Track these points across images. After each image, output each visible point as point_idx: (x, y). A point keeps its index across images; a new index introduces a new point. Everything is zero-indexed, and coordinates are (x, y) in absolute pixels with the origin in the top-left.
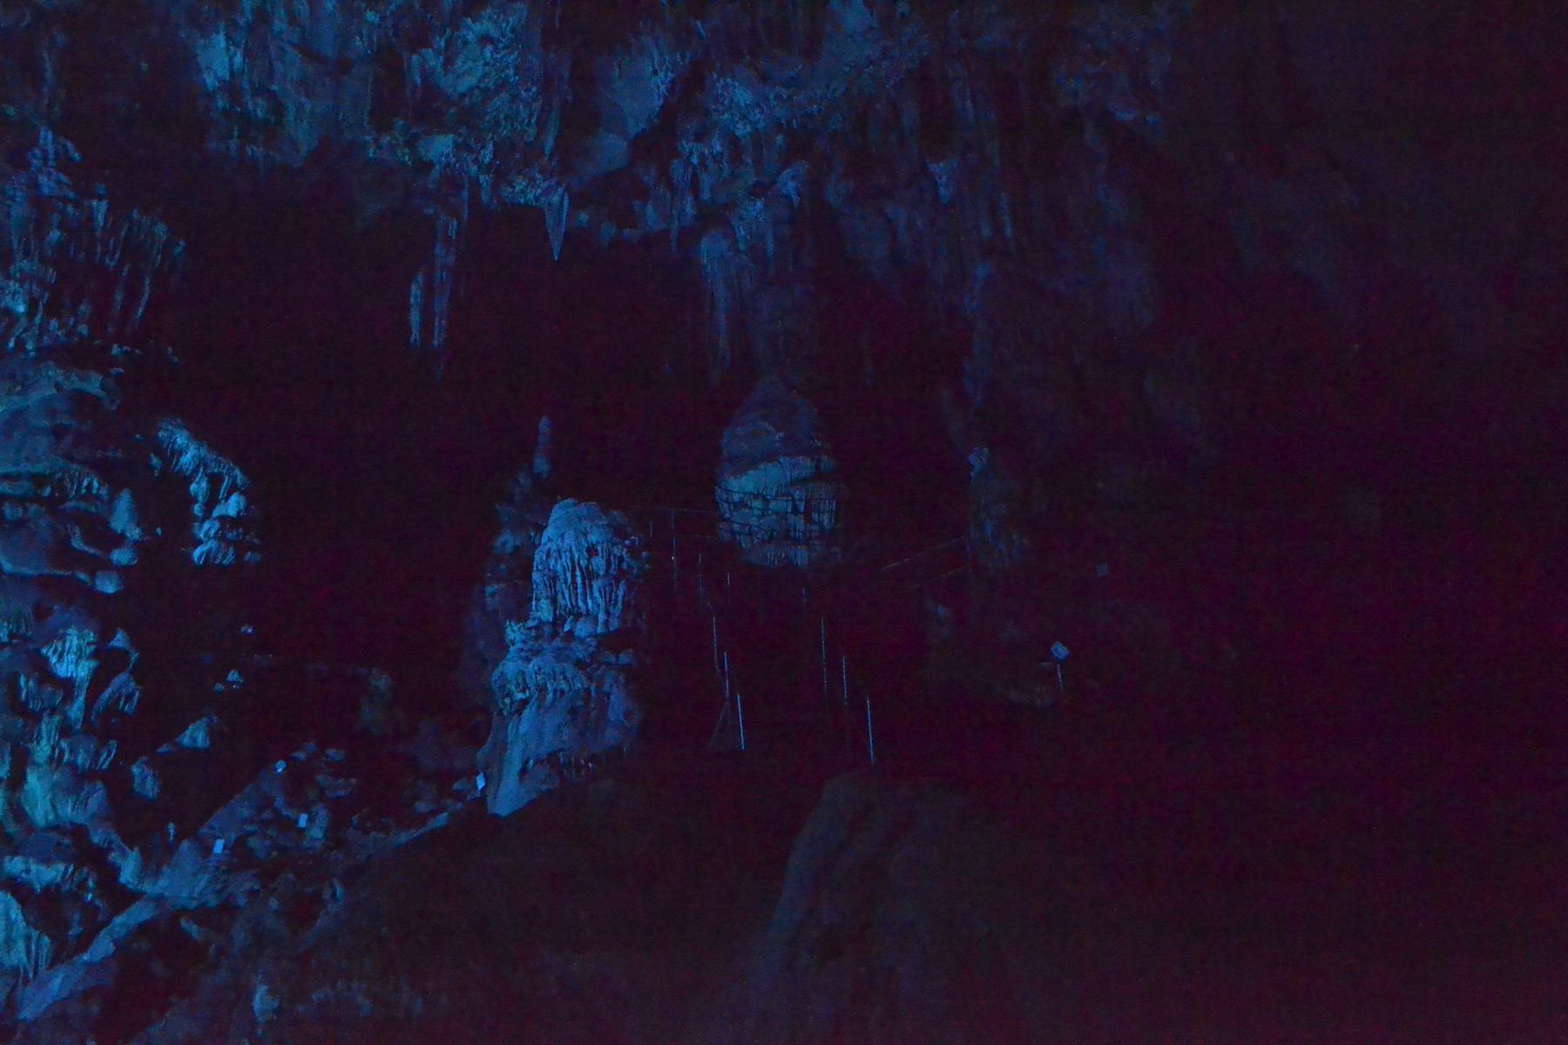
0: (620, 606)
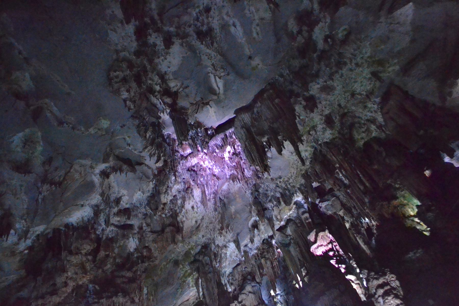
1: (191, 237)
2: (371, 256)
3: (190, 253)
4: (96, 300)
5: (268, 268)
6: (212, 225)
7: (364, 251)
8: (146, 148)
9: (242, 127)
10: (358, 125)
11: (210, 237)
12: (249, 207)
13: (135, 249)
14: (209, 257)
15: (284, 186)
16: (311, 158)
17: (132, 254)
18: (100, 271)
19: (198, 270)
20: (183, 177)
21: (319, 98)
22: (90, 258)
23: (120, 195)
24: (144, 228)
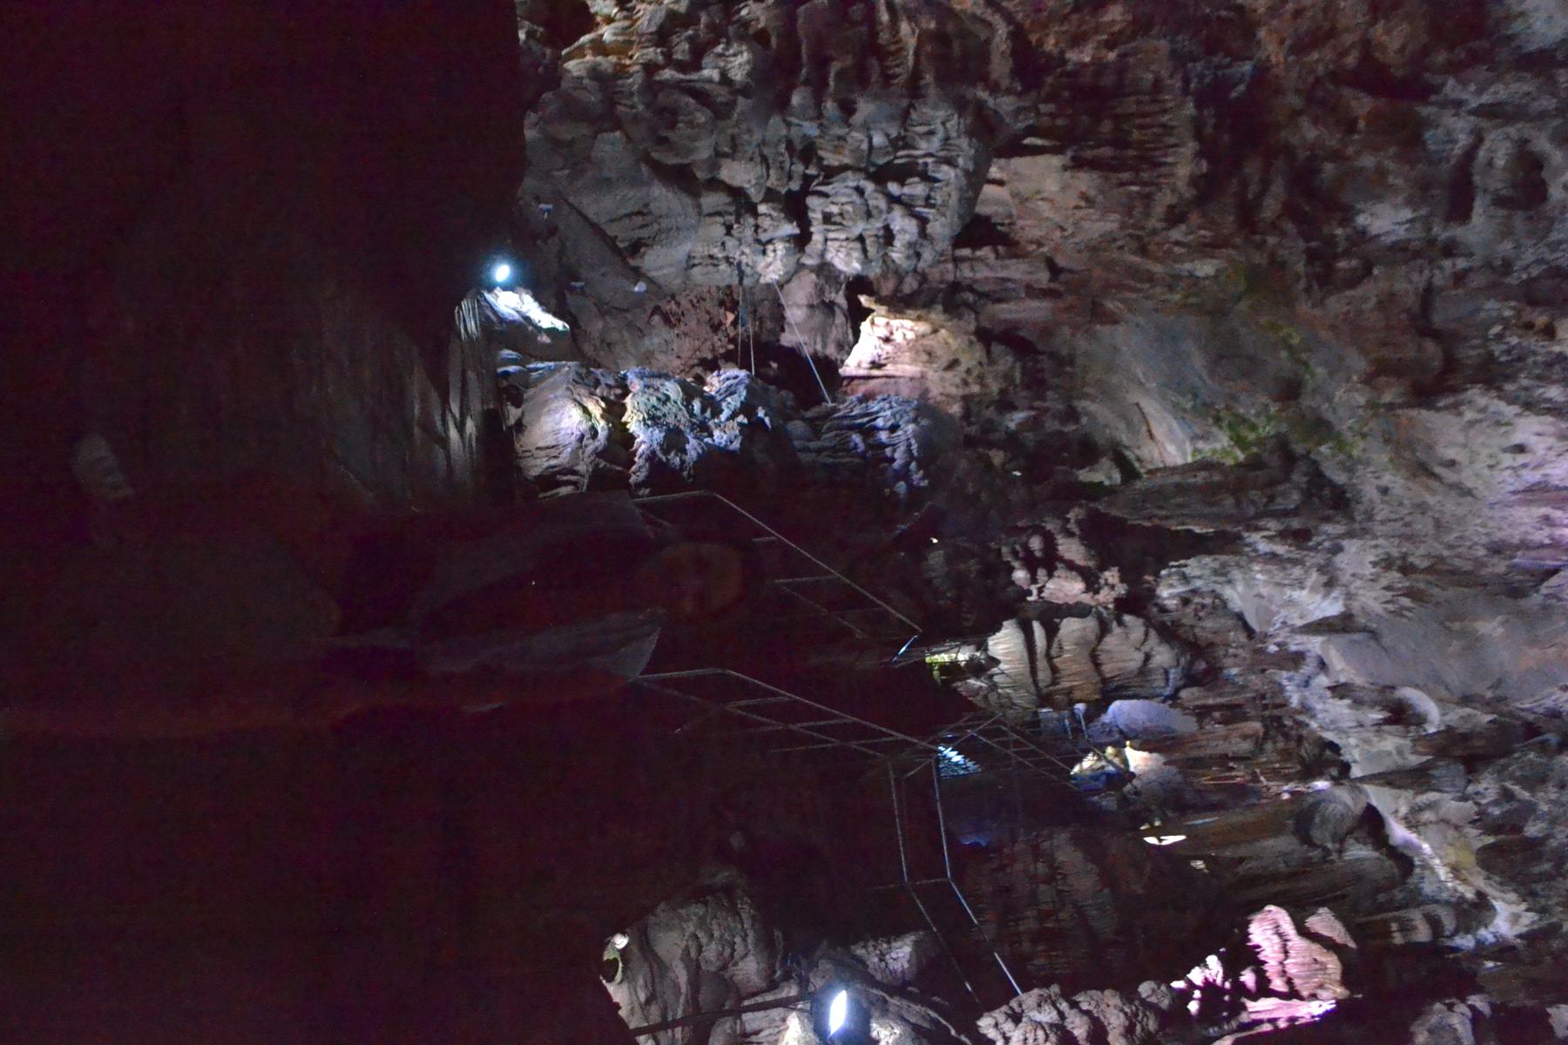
1: (1387, 441)
4: (1192, 85)
5: (1225, 738)
6: (1430, 529)
11: (1379, 518)
12: (1489, 694)
13: (1363, 233)
14: (1297, 508)
17: (1347, 214)
18: (1295, 101)
19: (1254, 464)
22: (1351, 60)
24: (1447, 263)
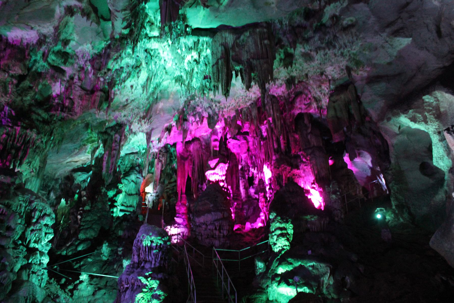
0: (159, 259)
2: (244, 200)
3: (105, 124)
4: (11, 125)
6: (137, 110)
7: (240, 193)
8: (125, 10)
9: (222, 45)
10: (305, 96)
11: (130, 119)
13: (58, 95)
15: (217, 110)
16: (254, 101)
18: (19, 98)
19: (105, 142)
20: (138, 55)
21: (296, 60)
23: (70, 38)
